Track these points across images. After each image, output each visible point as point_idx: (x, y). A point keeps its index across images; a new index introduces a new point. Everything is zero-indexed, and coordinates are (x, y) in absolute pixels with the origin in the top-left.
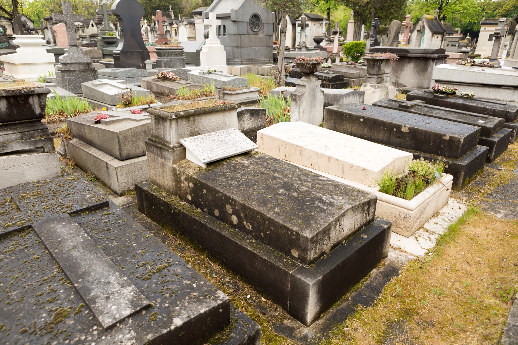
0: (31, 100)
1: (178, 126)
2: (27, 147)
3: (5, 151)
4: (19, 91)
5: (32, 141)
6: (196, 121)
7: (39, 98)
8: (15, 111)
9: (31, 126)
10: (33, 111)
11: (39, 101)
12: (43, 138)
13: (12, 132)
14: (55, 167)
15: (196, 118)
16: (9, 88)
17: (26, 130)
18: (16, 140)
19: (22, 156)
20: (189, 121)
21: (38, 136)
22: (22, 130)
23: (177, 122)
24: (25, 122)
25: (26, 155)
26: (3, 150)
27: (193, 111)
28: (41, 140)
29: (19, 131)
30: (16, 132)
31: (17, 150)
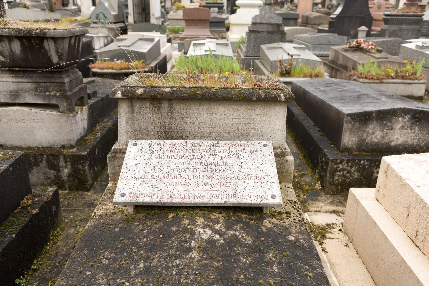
0: (46, 43)
1: (133, 113)
2: (40, 102)
3: (17, 101)
4: (30, 31)
5: (46, 95)
6: (176, 110)
7: (55, 43)
8: (30, 56)
9: (49, 77)
10: (49, 59)
11: (56, 47)
12: (58, 94)
13: (26, 81)
14: (67, 132)
15: (178, 107)
16: (19, 27)
17: (41, 81)
18: (30, 90)
19: (34, 110)
20: (159, 108)
21: (53, 90)
22: (37, 80)
23: (132, 106)
24: (32, 71)
25: (38, 110)
26: (15, 99)
27: (168, 90)
28: (55, 95)
29: (34, 80)
30: (30, 81)
31: (29, 102)
